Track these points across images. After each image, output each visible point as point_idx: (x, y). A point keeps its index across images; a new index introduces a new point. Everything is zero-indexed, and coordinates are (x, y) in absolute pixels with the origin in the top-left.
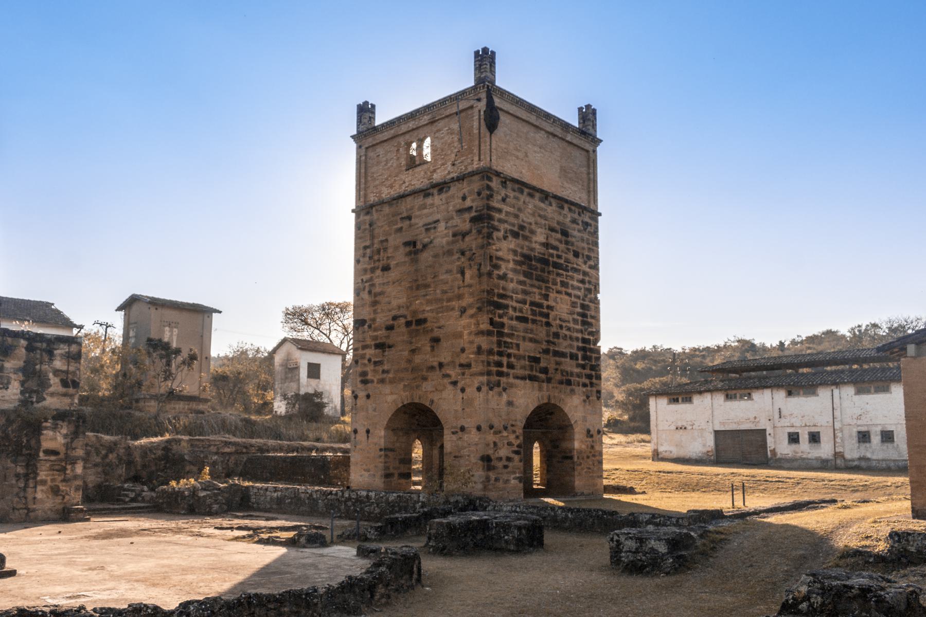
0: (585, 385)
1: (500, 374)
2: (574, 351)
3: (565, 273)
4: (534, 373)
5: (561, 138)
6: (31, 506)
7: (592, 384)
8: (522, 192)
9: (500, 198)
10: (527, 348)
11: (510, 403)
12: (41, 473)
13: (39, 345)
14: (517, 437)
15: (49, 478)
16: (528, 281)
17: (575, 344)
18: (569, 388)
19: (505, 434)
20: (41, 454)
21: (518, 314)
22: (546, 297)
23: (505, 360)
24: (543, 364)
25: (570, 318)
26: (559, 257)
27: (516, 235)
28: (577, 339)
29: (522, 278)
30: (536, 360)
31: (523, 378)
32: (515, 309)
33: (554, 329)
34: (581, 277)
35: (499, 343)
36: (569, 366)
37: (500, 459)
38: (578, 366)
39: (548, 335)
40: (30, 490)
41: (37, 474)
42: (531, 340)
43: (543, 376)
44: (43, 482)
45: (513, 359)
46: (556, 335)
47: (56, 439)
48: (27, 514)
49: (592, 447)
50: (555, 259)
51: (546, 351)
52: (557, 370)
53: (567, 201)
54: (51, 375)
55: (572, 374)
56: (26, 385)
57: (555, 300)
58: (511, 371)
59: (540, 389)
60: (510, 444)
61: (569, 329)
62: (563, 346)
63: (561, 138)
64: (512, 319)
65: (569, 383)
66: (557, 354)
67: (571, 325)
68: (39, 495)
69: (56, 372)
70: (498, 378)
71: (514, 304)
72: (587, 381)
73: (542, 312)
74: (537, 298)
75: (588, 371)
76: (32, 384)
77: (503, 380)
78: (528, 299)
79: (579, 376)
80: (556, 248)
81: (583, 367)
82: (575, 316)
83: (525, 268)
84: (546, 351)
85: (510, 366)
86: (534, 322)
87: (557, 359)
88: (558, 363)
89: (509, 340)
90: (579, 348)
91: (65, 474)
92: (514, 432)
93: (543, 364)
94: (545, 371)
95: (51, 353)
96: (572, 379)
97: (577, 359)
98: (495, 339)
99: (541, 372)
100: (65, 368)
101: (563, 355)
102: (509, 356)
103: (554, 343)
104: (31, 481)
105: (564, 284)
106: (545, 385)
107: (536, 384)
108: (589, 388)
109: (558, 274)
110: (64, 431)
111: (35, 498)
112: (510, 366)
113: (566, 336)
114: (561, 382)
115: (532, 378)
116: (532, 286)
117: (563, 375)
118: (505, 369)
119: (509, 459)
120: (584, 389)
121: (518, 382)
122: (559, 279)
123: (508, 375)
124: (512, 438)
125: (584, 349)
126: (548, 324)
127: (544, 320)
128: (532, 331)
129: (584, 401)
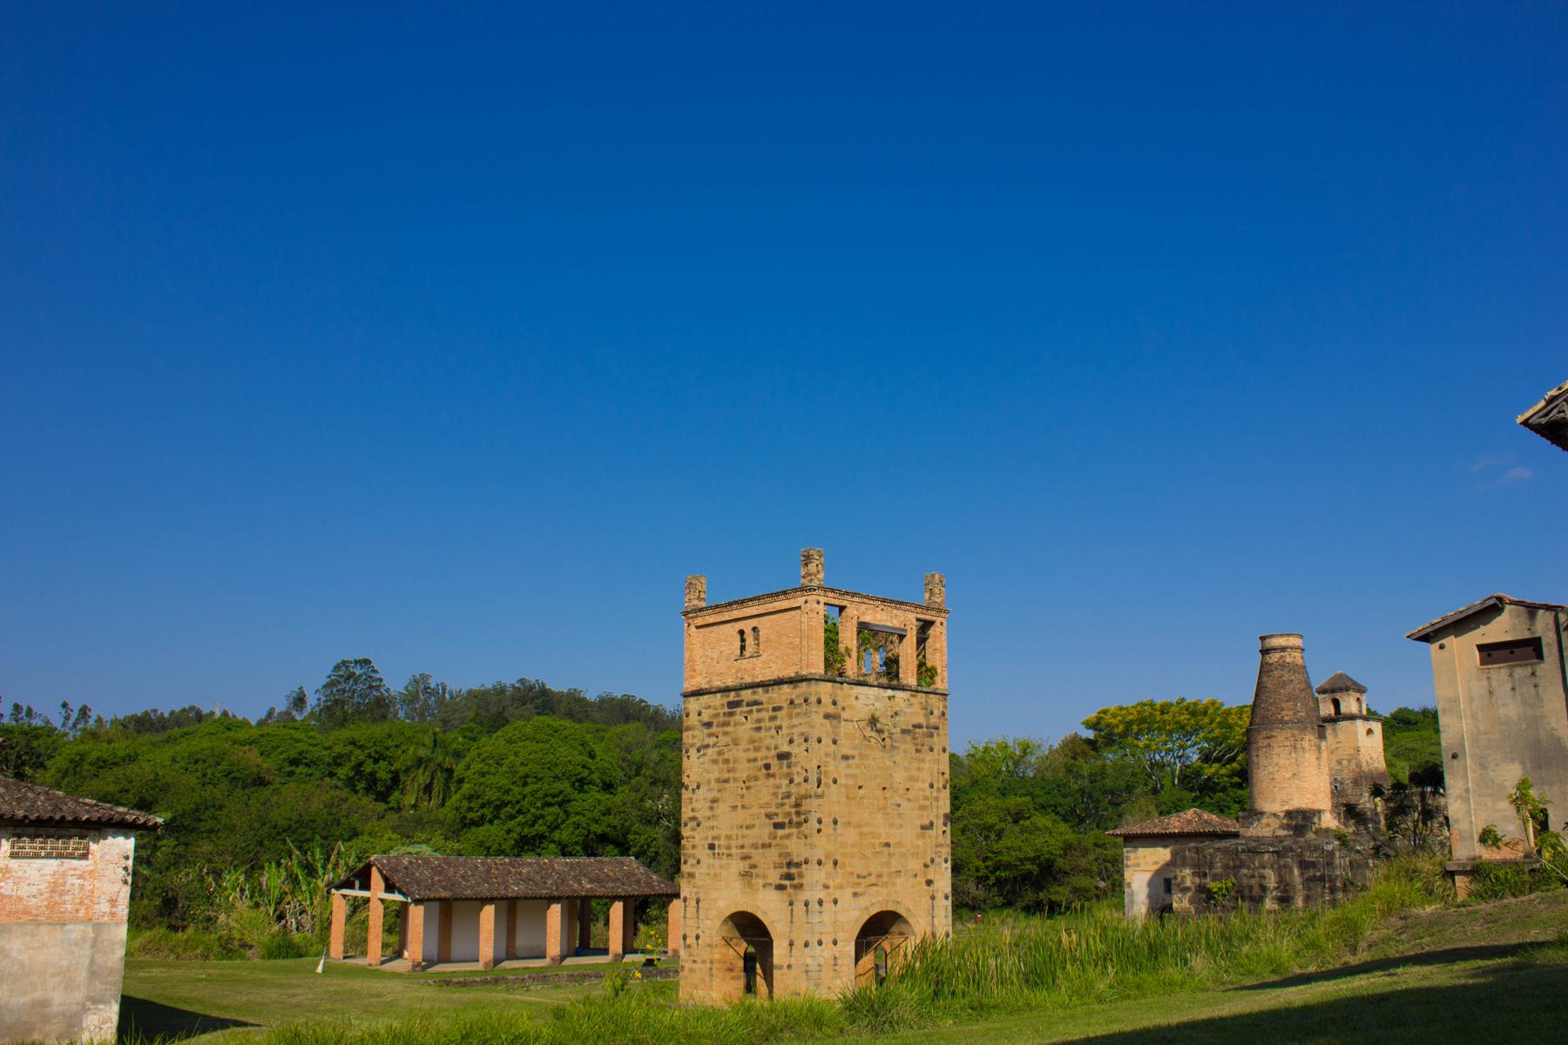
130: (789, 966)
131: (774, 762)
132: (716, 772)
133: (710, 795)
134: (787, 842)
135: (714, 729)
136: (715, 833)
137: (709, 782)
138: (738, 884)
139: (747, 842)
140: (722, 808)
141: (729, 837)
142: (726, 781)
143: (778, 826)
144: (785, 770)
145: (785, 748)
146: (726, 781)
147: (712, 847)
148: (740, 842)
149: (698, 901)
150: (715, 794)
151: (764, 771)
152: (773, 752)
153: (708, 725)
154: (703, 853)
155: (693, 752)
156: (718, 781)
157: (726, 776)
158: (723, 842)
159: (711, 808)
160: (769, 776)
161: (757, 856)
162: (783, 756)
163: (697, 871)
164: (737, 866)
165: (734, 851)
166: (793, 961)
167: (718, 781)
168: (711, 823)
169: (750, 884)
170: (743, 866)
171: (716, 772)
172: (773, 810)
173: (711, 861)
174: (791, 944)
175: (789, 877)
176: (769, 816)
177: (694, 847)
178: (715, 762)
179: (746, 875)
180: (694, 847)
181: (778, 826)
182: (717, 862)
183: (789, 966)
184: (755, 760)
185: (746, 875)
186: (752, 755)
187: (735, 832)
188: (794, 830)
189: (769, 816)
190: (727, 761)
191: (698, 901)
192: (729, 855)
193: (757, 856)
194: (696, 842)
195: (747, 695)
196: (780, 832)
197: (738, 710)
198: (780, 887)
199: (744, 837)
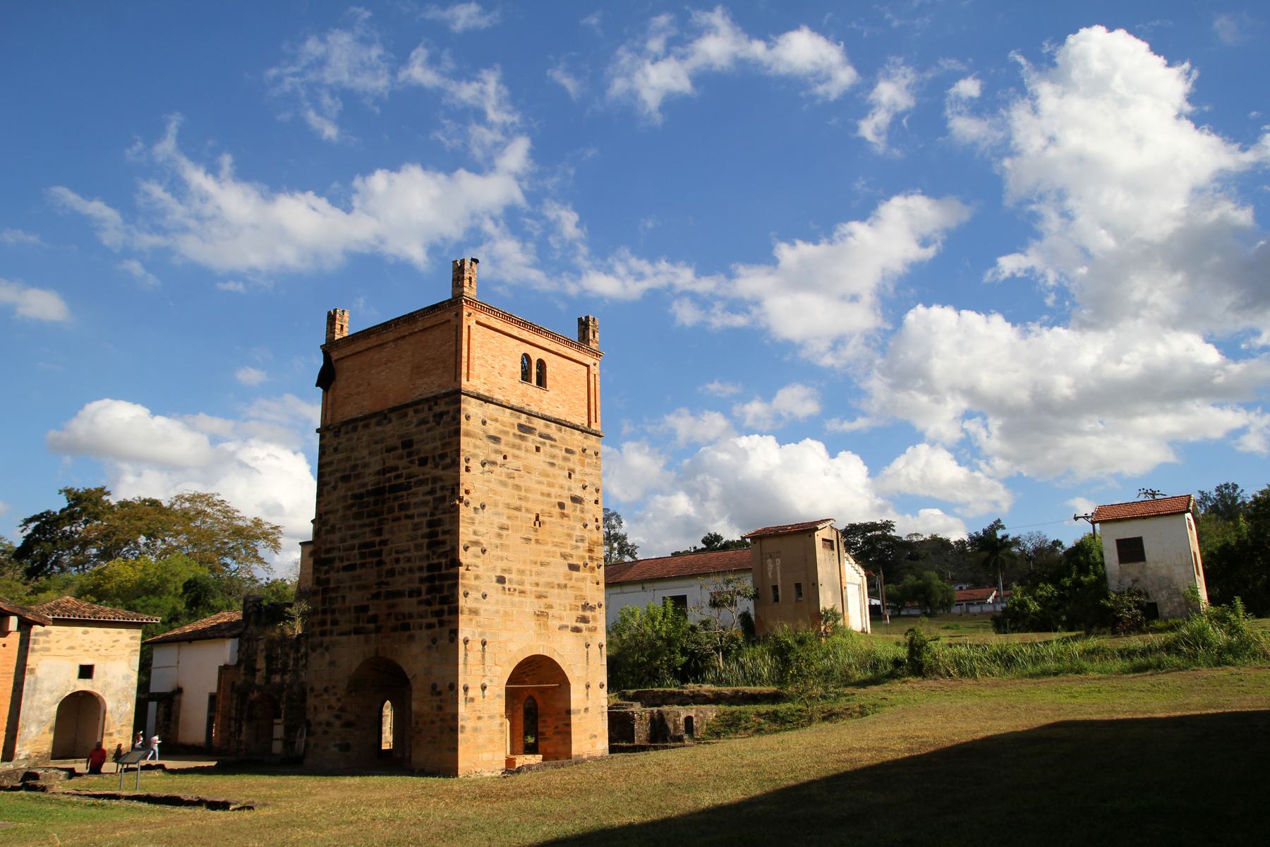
0: (430, 626)
1: (323, 634)
2: (415, 585)
3: (404, 493)
4: (361, 625)
5: (411, 334)
7: (441, 623)
8: (355, 429)
9: (331, 450)
10: (354, 598)
11: (332, 663)
14: (339, 700)
16: (358, 522)
17: (417, 575)
18: (408, 633)
19: (325, 697)
21: (346, 563)
22: (379, 532)
23: (329, 618)
24: (371, 612)
25: (411, 544)
26: (397, 477)
27: (345, 479)
28: (421, 569)
29: (352, 522)
30: (364, 609)
31: (348, 633)
32: (341, 559)
33: (388, 567)
34: (428, 488)
35: (324, 602)
36: (408, 605)
38: (420, 603)
39: (379, 576)
42: (360, 588)
43: (372, 626)
45: (337, 615)
46: (391, 573)
49: (440, 708)
50: (393, 482)
51: (377, 596)
52: (389, 615)
53: (407, 406)
55: (411, 616)
57: (392, 532)
59: (367, 641)
60: (330, 707)
61: (409, 560)
62: (399, 583)
63: (411, 334)
64: (338, 571)
65: (406, 627)
66: (391, 595)
67: (414, 553)
71: (341, 554)
72: (435, 620)
73: (372, 552)
74: (368, 538)
75: (436, 607)
77: (327, 639)
78: (356, 542)
79: (421, 616)
80: (396, 468)
81: (428, 603)
82: (420, 541)
83: (355, 509)
84: (377, 596)
85: (335, 623)
86: (363, 565)
87: (390, 601)
88: (393, 606)
89: (334, 595)
90: (422, 580)
93: (371, 612)
94: (374, 619)
96: (411, 621)
97: (419, 593)
98: (319, 598)
99: (369, 622)
101: (400, 594)
102: (333, 612)
103: (387, 584)
105: (403, 507)
106: (373, 636)
107: (362, 637)
108: (437, 629)
109: (396, 499)
112: (335, 623)
113: (404, 569)
114: (395, 629)
115: (357, 631)
116: (362, 526)
117: (397, 619)
118: (328, 627)
119: (329, 724)
120: (429, 632)
121: (344, 638)
122: (396, 504)
123: (331, 633)
124: (333, 702)
125: (431, 579)
126: (380, 563)
127: (375, 559)
128: (360, 577)
129: (429, 648)
130: (586, 710)
131: (568, 503)
132: (507, 496)
133: (498, 521)
134: (582, 585)
135: (502, 447)
136: (505, 564)
137: (496, 505)
138: (532, 623)
139: (542, 580)
140: (513, 538)
141: (522, 572)
142: (518, 509)
143: (574, 568)
144: (578, 513)
145: (578, 492)
146: (518, 509)
147: (501, 580)
148: (535, 579)
149: (484, 643)
150: (505, 521)
151: (557, 510)
152: (566, 493)
153: (496, 439)
154: (493, 588)
155: (475, 464)
156: (508, 506)
157: (517, 503)
158: (514, 576)
159: (500, 536)
160: (563, 515)
161: (555, 597)
162: (576, 500)
163: (483, 606)
164: (531, 605)
165: (527, 587)
166: (589, 704)
167: (508, 506)
168: (499, 552)
169: (546, 626)
170: (539, 605)
171: (507, 496)
172: (568, 551)
173: (501, 597)
174: (588, 687)
175: (584, 620)
176: (564, 556)
177: (477, 577)
178: (504, 484)
179: (541, 615)
180: (477, 577)
181: (574, 568)
182: (507, 597)
183: (586, 710)
184: (549, 495)
185: (541, 615)
186: (546, 489)
187: (528, 567)
188: (587, 574)
189: (564, 556)
190: (518, 487)
191: (484, 643)
192: (522, 592)
193: (555, 597)
194: (480, 571)
195: (539, 424)
196: (575, 574)
197: (530, 437)
198: (576, 630)
199: (538, 574)
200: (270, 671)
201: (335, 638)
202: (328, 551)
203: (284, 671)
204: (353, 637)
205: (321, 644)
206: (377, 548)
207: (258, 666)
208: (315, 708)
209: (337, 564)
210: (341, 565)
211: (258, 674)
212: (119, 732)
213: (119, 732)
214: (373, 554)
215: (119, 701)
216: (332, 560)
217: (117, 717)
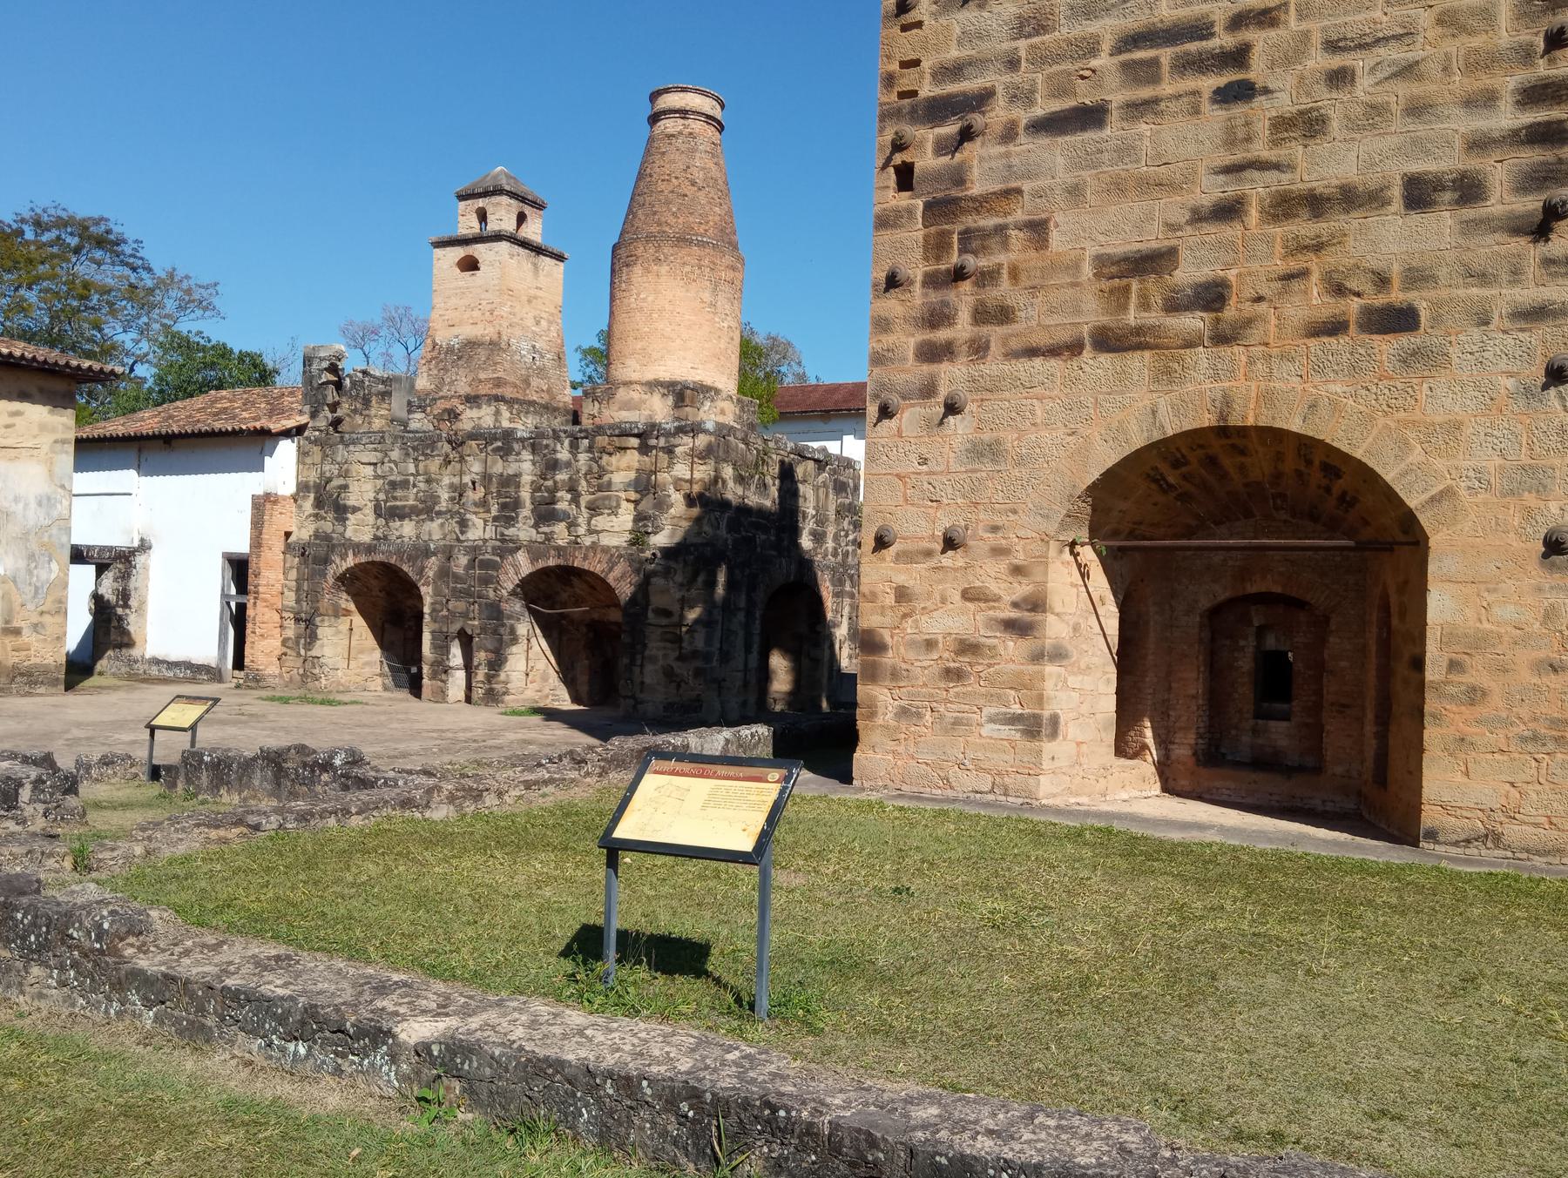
4: (1132, 317)
6: (641, 696)
10: (1090, 232)
11: (985, 451)
12: (650, 645)
13: (653, 442)
15: (660, 653)
20: (650, 615)
23: (964, 298)
32: (1022, 96)
35: (936, 246)
37: (930, 644)
40: (637, 670)
41: (645, 646)
43: (1194, 322)
44: (653, 660)
47: (668, 590)
48: (634, 707)
54: (671, 490)
56: (640, 508)
58: (995, 333)
65: (1400, 320)
68: (648, 680)
69: (677, 482)
70: (926, 368)
76: (647, 505)
91: (681, 648)
92: (998, 552)
93: (1187, 274)
94: (1212, 296)
95: (669, 451)
100: (688, 477)
102: (987, 277)
104: (639, 657)
106: (1201, 356)
107: (1139, 363)
110: (679, 578)
111: (642, 683)
115: (1107, 341)
119: (967, 648)
123: (979, 349)
200: (388, 512)
201: (993, 366)
202: (954, 71)
203: (427, 509)
204: (1096, 365)
205: (928, 390)
206: (1223, 40)
207: (351, 500)
208: (902, 594)
209: (999, 113)
210: (1023, 116)
211: (352, 519)
212: (36, 627)
213: (36, 627)
214: (1198, 64)
215: (31, 557)
216: (982, 99)
217: (29, 591)
